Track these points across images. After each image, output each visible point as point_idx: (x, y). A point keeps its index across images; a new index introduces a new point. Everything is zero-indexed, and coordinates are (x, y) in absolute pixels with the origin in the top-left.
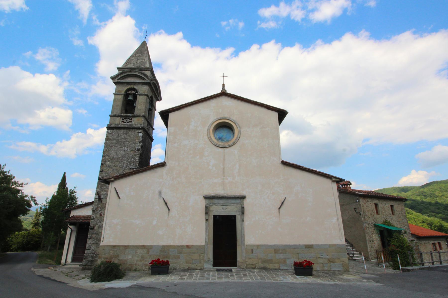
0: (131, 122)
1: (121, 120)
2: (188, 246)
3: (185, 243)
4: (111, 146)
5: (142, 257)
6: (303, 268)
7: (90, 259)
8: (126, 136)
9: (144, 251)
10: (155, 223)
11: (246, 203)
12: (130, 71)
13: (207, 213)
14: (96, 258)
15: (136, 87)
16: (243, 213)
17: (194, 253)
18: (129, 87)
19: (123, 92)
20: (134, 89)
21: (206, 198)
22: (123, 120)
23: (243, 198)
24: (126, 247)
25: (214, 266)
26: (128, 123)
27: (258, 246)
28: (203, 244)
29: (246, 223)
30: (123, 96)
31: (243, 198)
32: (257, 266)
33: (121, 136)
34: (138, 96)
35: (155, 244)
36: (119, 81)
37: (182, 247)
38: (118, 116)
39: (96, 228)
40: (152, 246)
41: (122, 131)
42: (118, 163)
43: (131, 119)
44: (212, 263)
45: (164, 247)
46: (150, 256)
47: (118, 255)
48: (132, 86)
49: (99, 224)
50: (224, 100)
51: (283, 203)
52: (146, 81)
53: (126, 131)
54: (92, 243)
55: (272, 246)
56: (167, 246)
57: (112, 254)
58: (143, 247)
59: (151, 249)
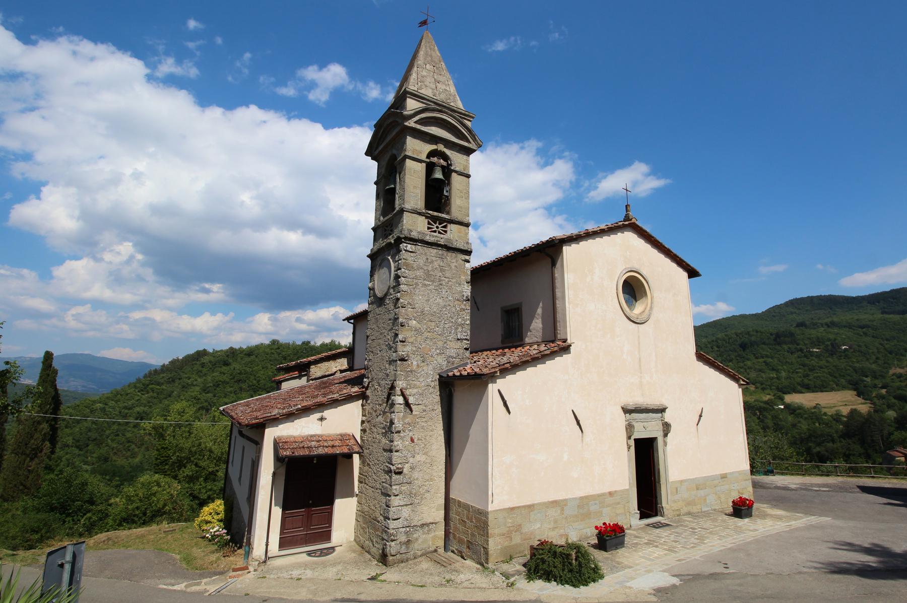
0: (446, 232)
1: (427, 225)
2: (611, 494)
3: (606, 490)
4: (417, 284)
5: (556, 521)
6: (741, 509)
7: (403, 538)
8: (441, 264)
9: (553, 513)
10: (566, 457)
11: (668, 416)
12: (440, 111)
13: (629, 438)
14: (415, 536)
15: (448, 152)
16: (666, 435)
17: (619, 503)
18: (434, 147)
19: (423, 157)
20: (445, 158)
21: (626, 411)
22: (429, 223)
23: (662, 410)
24: (531, 507)
25: (641, 518)
26: (439, 233)
27: (682, 481)
28: (627, 487)
29: (669, 447)
30: (424, 165)
31: (662, 410)
32: (682, 512)
33: (432, 262)
34: (454, 175)
35: (570, 496)
36: (418, 127)
37: (603, 495)
38: (420, 214)
39: (405, 471)
40: (566, 500)
41: (433, 251)
42: (433, 324)
43: (445, 227)
44: (638, 516)
45: (581, 498)
46: (566, 518)
47: (520, 525)
48: (441, 147)
49: (411, 460)
50: (630, 238)
51: (701, 416)
52: (470, 146)
53: (440, 252)
54: (402, 503)
55: (693, 479)
56: (586, 497)
57: (510, 525)
58: (555, 503)
59: (565, 505)
